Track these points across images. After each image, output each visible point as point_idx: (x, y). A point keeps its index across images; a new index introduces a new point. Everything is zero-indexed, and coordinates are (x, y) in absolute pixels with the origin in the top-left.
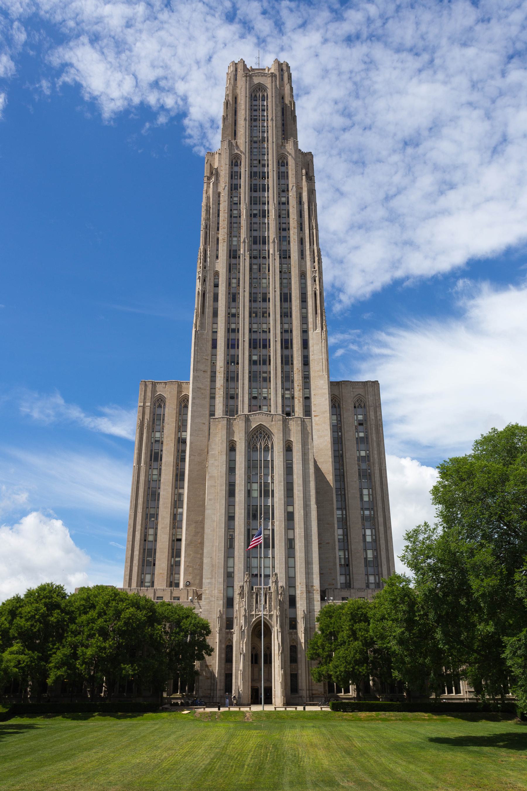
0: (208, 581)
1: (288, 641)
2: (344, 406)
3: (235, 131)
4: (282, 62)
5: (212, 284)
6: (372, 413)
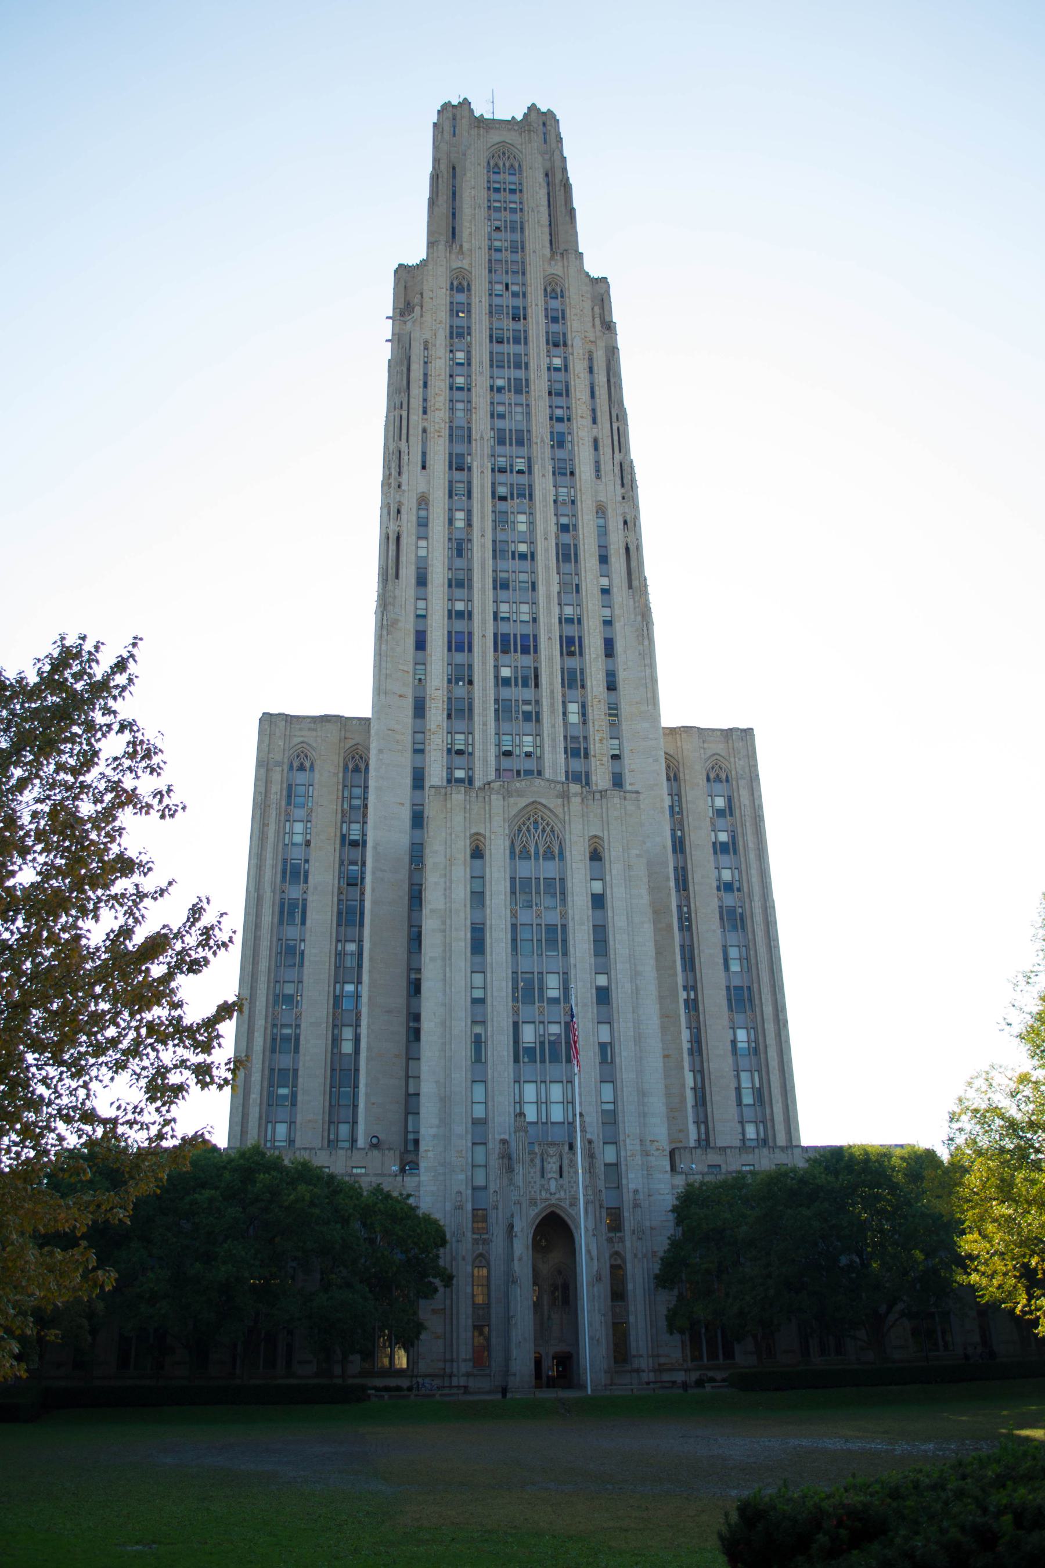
0: (433, 1131)
1: (607, 1256)
2: (687, 777)
3: (454, 229)
6: (744, 793)
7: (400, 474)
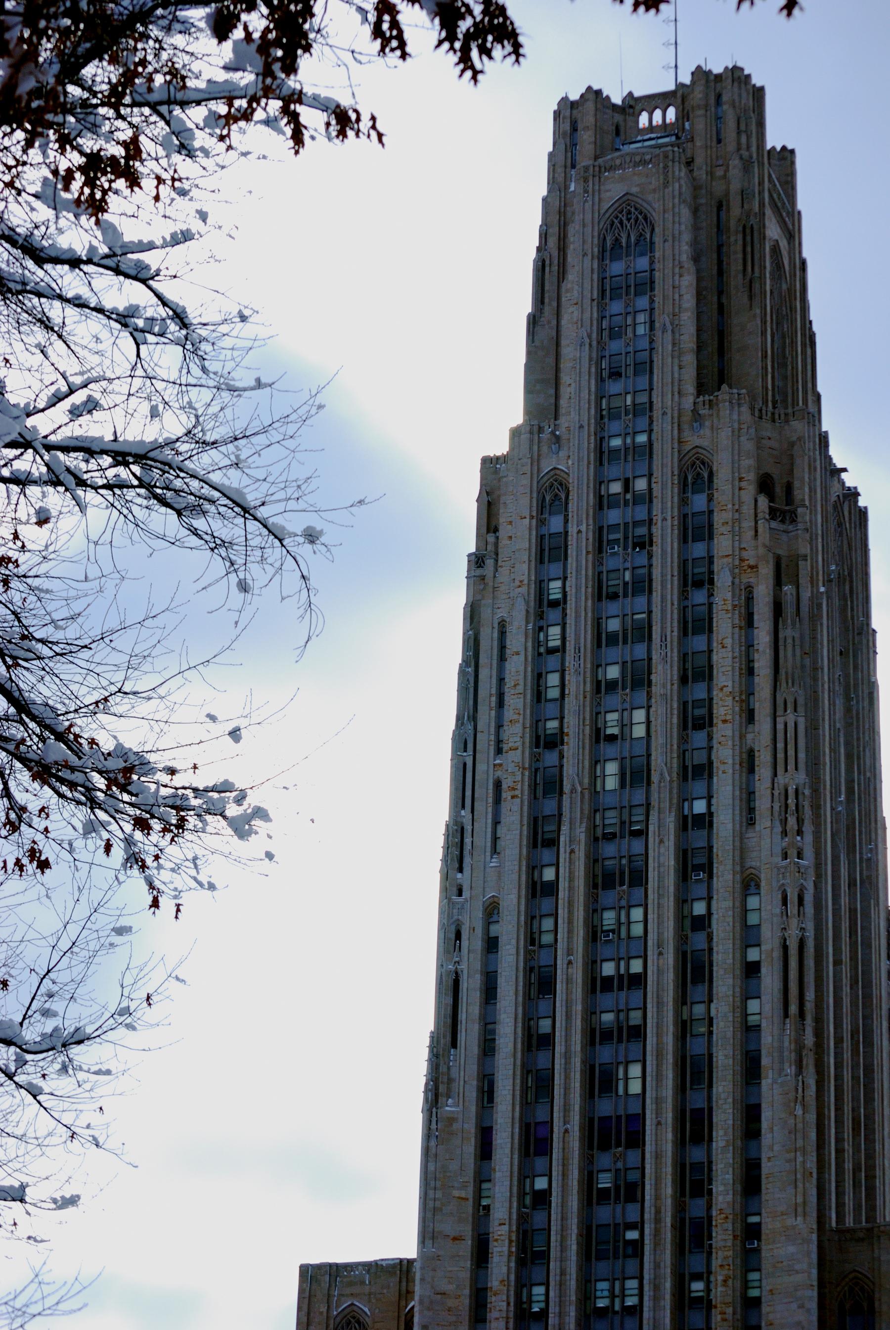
4: (718, 69)
5: (478, 944)
7: (461, 870)
